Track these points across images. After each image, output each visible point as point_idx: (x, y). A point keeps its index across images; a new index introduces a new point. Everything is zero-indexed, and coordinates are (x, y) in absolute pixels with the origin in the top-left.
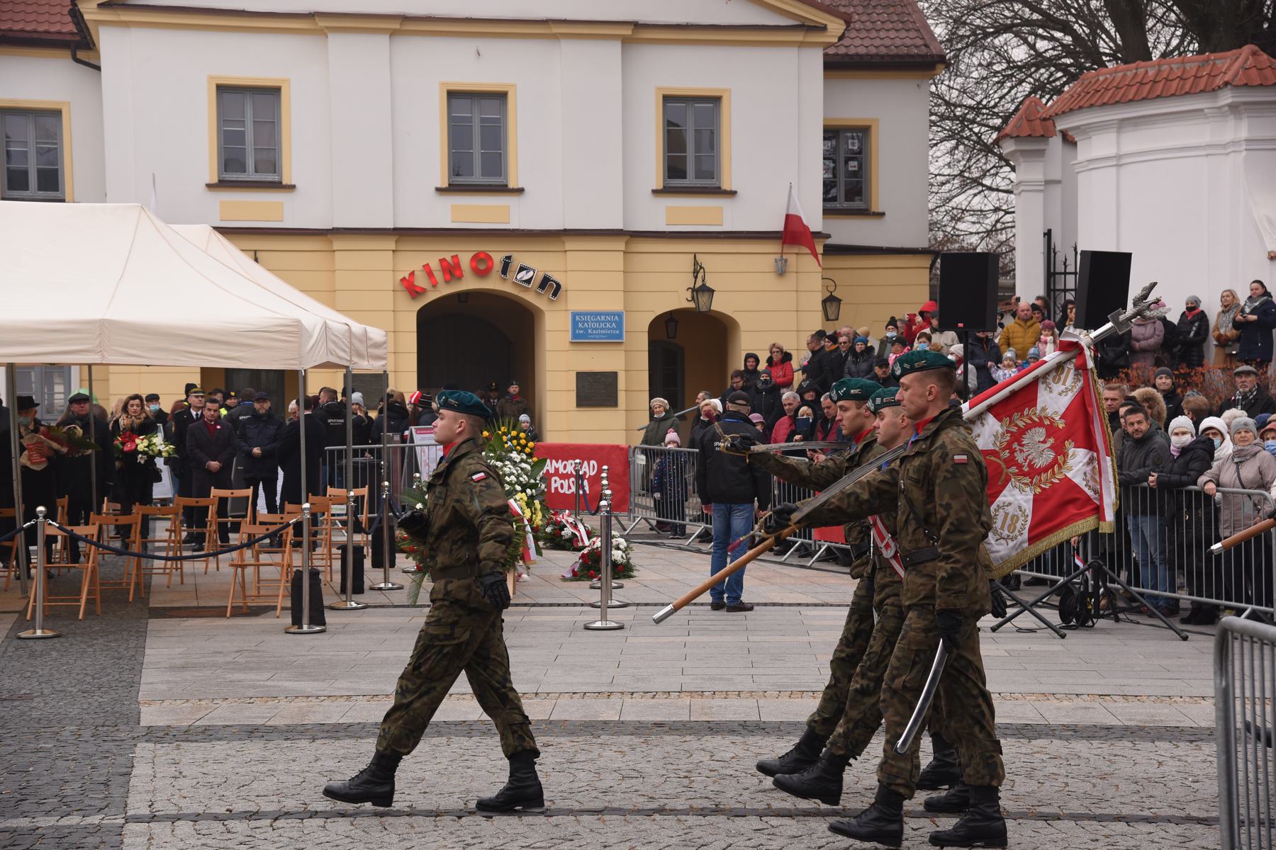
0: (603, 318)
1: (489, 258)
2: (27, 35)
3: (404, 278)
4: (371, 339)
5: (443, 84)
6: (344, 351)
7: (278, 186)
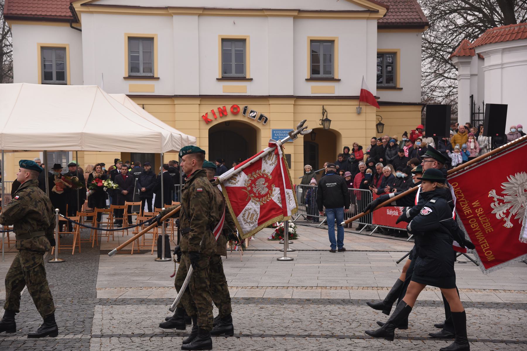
0: (285, 132)
2: (52, 17)
3: (204, 115)
4: (190, 141)
5: (219, 36)
6: (179, 145)
7: (152, 78)
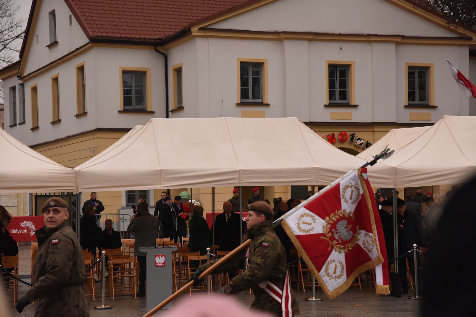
1: (346, 134)
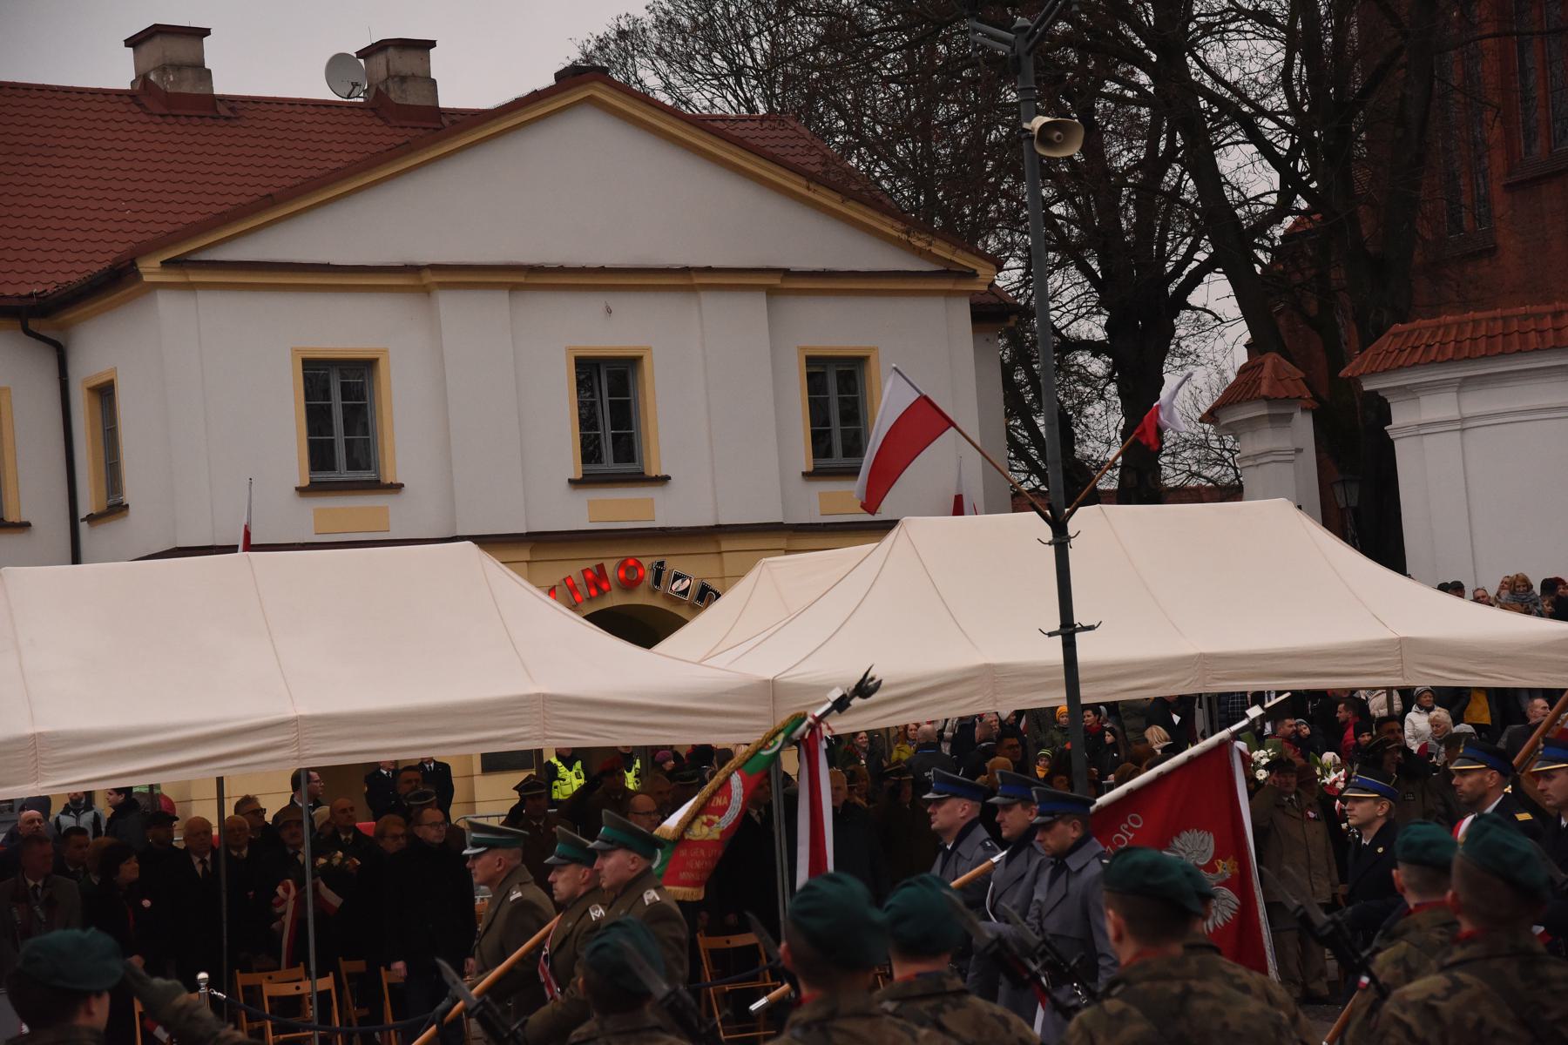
1: (640, 564)
7: (377, 486)
